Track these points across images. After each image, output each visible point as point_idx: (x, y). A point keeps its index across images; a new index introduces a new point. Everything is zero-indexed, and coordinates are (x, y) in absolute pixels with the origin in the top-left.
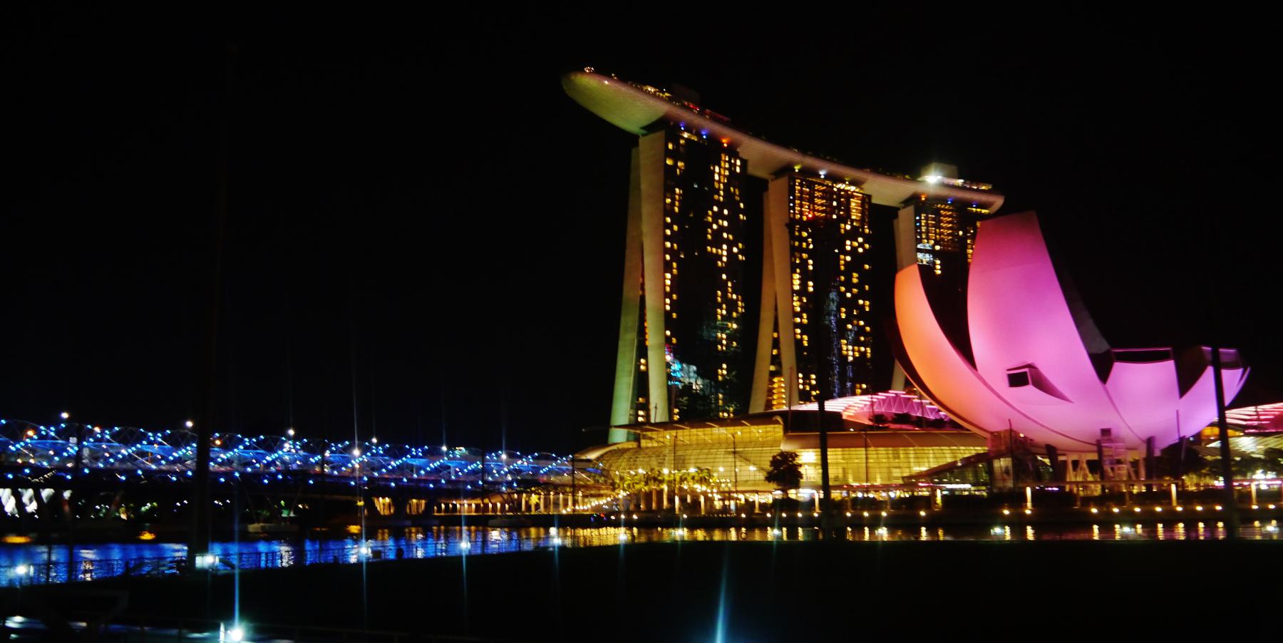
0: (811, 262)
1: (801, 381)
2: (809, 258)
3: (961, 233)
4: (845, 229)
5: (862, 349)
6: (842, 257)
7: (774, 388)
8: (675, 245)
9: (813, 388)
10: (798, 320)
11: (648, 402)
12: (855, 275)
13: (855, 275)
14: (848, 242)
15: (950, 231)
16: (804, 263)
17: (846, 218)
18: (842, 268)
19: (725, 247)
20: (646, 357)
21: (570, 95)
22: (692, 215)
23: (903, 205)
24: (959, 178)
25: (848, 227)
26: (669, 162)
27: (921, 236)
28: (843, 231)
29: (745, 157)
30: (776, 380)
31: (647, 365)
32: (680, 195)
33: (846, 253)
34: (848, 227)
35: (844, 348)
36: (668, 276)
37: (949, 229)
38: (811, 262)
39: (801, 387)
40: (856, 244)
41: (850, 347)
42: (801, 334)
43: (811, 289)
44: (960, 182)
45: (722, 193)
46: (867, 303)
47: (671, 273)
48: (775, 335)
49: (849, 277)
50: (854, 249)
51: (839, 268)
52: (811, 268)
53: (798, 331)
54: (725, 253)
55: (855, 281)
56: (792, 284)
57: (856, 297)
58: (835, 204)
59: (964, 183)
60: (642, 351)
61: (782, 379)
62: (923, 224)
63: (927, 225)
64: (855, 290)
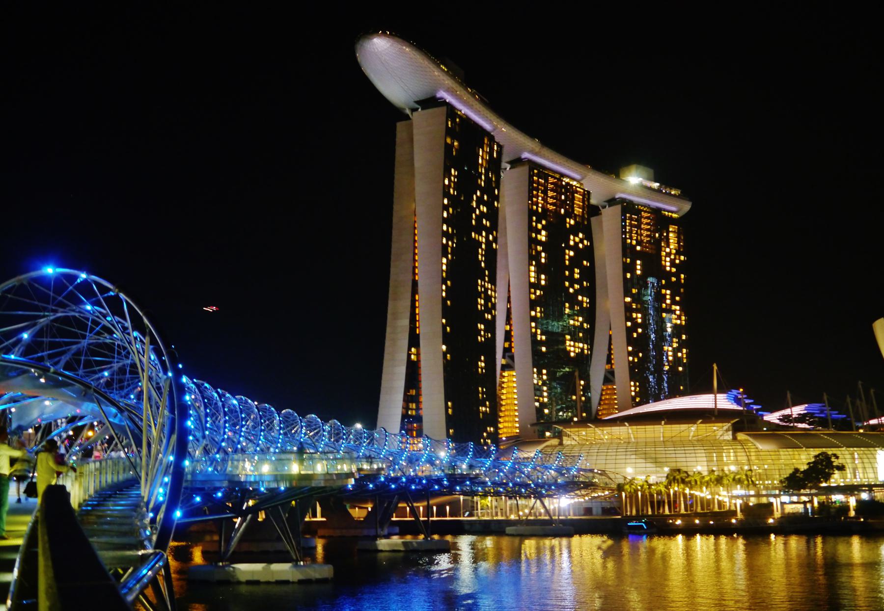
0: (543, 255)
1: (535, 376)
2: (543, 251)
3: (657, 235)
4: (569, 223)
5: (581, 345)
6: (567, 251)
7: (503, 382)
8: (450, 230)
9: (544, 384)
10: (533, 313)
11: (419, 394)
12: (577, 271)
13: (577, 271)
14: (572, 237)
15: (649, 233)
16: (539, 253)
17: (570, 214)
18: (567, 262)
19: (484, 234)
20: (417, 346)
21: (359, 59)
22: (462, 199)
23: (606, 203)
24: (656, 181)
25: (572, 222)
26: (449, 141)
27: (626, 236)
28: (568, 225)
29: (501, 144)
30: (506, 374)
31: (418, 354)
32: (455, 176)
33: (570, 248)
34: (572, 222)
35: (568, 343)
36: (444, 260)
37: (647, 230)
38: (543, 255)
39: (535, 382)
40: (577, 239)
41: (572, 343)
42: (536, 328)
43: (543, 283)
44: (656, 185)
45: (483, 177)
46: (585, 299)
47: (447, 258)
48: (508, 328)
49: (572, 273)
50: (576, 244)
51: (565, 263)
52: (543, 261)
53: (533, 324)
54: (484, 240)
55: (577, 276)
56: (529, 277)
57: (577, 292)
58: (563, 197)
59: (660, 186)
60: (414, 340)
61: (514, 374)
62: (628, 224)
63: (631, 225)
64: (577, 286)
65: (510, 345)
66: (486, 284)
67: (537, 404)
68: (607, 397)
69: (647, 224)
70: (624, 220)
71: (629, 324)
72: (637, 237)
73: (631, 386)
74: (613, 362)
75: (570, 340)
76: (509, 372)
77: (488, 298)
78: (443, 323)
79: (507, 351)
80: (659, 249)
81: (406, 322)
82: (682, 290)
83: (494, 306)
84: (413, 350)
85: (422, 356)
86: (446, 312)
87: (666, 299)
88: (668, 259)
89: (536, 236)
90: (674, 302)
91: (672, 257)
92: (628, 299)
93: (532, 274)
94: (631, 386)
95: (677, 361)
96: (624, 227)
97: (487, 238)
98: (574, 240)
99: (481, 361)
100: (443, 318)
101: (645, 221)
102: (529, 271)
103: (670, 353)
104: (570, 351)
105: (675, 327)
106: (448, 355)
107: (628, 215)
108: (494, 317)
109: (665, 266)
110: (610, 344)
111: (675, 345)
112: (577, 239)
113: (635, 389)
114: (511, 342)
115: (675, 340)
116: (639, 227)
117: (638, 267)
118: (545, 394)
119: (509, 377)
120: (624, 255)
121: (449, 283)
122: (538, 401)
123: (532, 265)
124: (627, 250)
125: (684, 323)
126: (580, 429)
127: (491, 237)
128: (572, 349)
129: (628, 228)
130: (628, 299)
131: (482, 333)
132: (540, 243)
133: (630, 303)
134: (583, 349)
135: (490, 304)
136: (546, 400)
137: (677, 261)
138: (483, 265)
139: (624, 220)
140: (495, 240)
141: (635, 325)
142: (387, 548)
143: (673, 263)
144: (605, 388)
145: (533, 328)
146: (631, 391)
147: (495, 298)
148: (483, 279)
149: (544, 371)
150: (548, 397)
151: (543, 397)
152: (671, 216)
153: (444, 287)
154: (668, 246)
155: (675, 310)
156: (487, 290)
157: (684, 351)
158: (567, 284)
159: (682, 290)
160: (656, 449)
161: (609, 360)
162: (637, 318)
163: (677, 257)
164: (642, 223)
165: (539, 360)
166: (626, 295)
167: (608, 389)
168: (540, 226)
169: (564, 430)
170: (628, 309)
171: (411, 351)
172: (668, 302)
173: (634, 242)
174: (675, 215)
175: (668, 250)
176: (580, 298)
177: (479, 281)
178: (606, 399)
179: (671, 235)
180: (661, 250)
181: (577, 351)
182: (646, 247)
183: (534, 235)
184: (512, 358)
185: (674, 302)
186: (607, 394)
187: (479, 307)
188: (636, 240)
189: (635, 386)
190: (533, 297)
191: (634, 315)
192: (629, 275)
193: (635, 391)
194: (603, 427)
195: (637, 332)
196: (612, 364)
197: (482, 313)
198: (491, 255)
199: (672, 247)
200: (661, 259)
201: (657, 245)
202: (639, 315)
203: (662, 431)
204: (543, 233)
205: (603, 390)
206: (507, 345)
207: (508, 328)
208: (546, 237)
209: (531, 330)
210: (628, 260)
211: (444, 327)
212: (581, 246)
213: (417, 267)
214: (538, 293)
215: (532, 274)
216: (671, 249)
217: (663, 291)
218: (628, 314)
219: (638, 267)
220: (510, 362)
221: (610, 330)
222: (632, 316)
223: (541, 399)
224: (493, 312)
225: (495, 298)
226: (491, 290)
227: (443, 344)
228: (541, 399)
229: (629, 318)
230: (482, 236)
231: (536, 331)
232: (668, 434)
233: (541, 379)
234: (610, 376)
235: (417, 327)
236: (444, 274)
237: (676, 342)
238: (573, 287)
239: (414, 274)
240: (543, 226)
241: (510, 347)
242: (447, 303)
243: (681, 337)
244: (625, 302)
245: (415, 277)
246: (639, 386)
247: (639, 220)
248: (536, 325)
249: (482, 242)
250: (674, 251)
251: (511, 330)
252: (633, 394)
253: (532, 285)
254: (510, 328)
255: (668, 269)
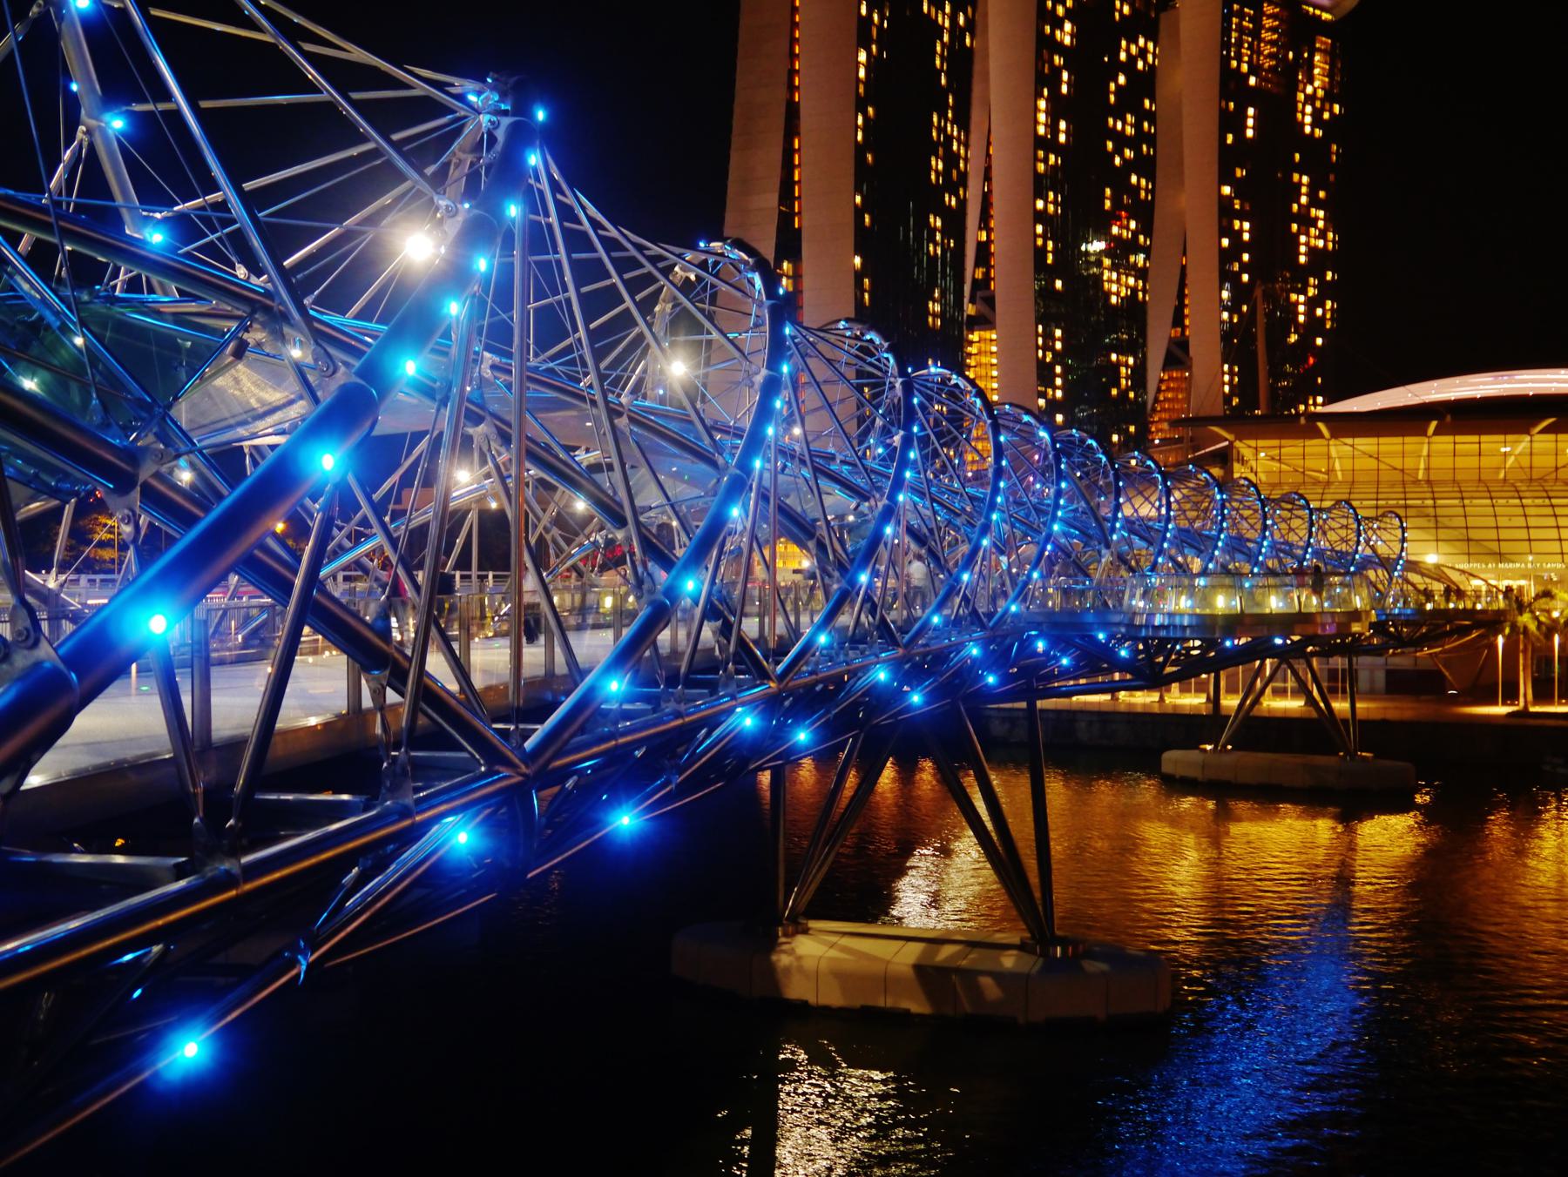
0: (1065, 76)
2: (1065, 67)
3: (1291, 55)
4: (1121, 11)
10: (1040, 204)
14: (1124, 43)
16: (1057, 72)
18: (1112, 98)
27: (1229, 52)
28: (1117, 15)
34: (1126, 10)
35: (1106, 275)
36: (862, 57)
37: (1272, 43)
38: (1065, 76)
42: (1044, 237)
43: (1062, 138)
50: (1132, 59)
51: (1108, 99)
52: (1064, 89)
54: (947, 24)
56: (1036, 122)
61: (994, 337)
63: (1241, 29)
64: (1128, 153)
65: (987, 275)
66: (949, 125)
67: (1042, 402)
68: (1170, 395)
69: (1273, 30)
70: (1226, 19)
71: (1225, 242)
72: (1250, 57)
73: (1223, 373)
74: (1187, 322)
75: (1111, 270)
76: (982, 333)
77: (951, 160)
78: (855, 205)
79: (981, 285)
80: (1294, 87)
81: (771, 200)
82: (1332, 177)
83: (963, 177)
84: (785, 265)
85: (807, 282)
86: (862, 177)
87: (1300, 194)
88: (1309, 109)
89: (1053, 32)
90: (1315, 202)
91: (1318, 104)
92: (1226, 190)
93: (1042, 117)
94: (1223, 373)
95: (1315, 325)
96: (1226, 31)
97: (954, 19)
98: (1128, 51)
99: (934, 301)
100: (858, 190)
101: (1268, 23)
102: (1036, 110)
103: (1301, 308)
104: (1109, 293)
105: (1312, 251)
106: (866, 281)
107: (1236, 7)
108: (962, 203)
109: (1302, 124)
110: (1182, 285)
111: (1311, 292)
112: (1133, 49)
113: (1231, 380)
114: (989, 267)
115: (1311, 280)
116: (1256, 34)
117: (1250, 122)
118: (1059, 381)
119: (983, 345)
120: (1225, 95)
121: (870, 110)
122: (1043, 395)
123: (1042, 96)
124: (1231, 83)
125: (1330, 246)
126: (1284, 442)
127: (961, 20)
128: (1114, 288)
129: (1234, 35)
130: (1226, 190)
131: (938, 237)
132: (1059, 48)
133: (1229, 199)
134: (1134, 290)
135: (955, 173)
136: (1059, 394)
137: (1326, 115)
138: (943, 81)
139: (1226, 19)
140: (971, 26)
141: (1238, 246)
142: (832, 997)
143: (1317, 121)
144: (1166, 377)
145: (1040, 236)
146: (1224, 383)
147: (966, 160)
148: (942, 115)
149: (1058, 333)
150: (1063, 388)
151: (1055, 388)
152: (1320, 16)
153: (860, 121)
154: (1311, 80)
155: (1317, 219)
156: (949, 138)
157: (1329, 304)
158: (1110, 145)
159: (1332, 177)
160: (1439, 502)
161: (1178, 320)
162: (1241, 231)
163: (1327, 106)
164: (1263, 27)
165: (1049, 309)
166: (1222, 182)
167: (1171, 379)
168: (1060, 10)
169: (1237, 444)
170: (1226, 211)
171: (781, 268)
172: (1304, 200)
173: (1245, 68)
174: (1326, 16)
175: (1309, 90)
176: (1134, 179)
177: (935, 119)
178: (1166, 399)
179: (1317, 58)
180: (1296, 90)
181: (1123, 294)
182: (1266, 80)
183: (1048, 29)
184: (990, 301)
185: (1315, 202)
186: (1168, 389)
187: (933, 177)
188: (1250, 63)
189: (1231, 373)
190: (1041, 167)
191: (1237, 224)
192: (1230, 139)
193: (1231, 383)
194: (1353, 436)
195: (1240, 260)
196: (1184, 328)
197: (938, 191)
198: (962, 61)
199: (1317, 84)
200: (1296, 107)
201: (1288, 76)
202: (1246, 226)
203: (1425, 452)
204: (1068, 26)
205: (1162, 381)
206: (979, 274)
207: (983, 236)
208: (1072, 35)
209: (1035, 241)
210: (1232, 105)
211: (859, 213)
212: (1140, 65)
213: (798, 72)
214: (1052, 158)
215: (1042, 117)
216: (1315, 89)
217: (1296, 177)
218: (1225, 223)
219: (1250, 122)
220: (985, 310)
221: (1185, 254)
222: (1232, 225)
223: (1050, 391)
224: (961, 192)
225: (966, 160)
226: (959, 143)
227: (856, 253)
228: (1050, 391)
229: (1226, 230)
230: (944, 14)
231: (1045, 244)
232: (1544, 462)
233: (1052, 349)
234: (1179, 353)
235: (795, 214)
236: (861, 90)
237: (1314, 286)
238: (1122, 155)
239: (792, 88)
240: (1067, 10)
241: (987, 278)
242: (866, 158)
243: (1325, 275)
244: (1221, 196)
245: (792, 96)
246: (1238, 374)
247: (1257, 20)
248: (1045, 231)
249: (943, 27)
250: (1320, 93)
251: (989, 241)
252: (1227, 389)
253: (1040, 142)
254: (988, 236)
255: (1308, 130)
